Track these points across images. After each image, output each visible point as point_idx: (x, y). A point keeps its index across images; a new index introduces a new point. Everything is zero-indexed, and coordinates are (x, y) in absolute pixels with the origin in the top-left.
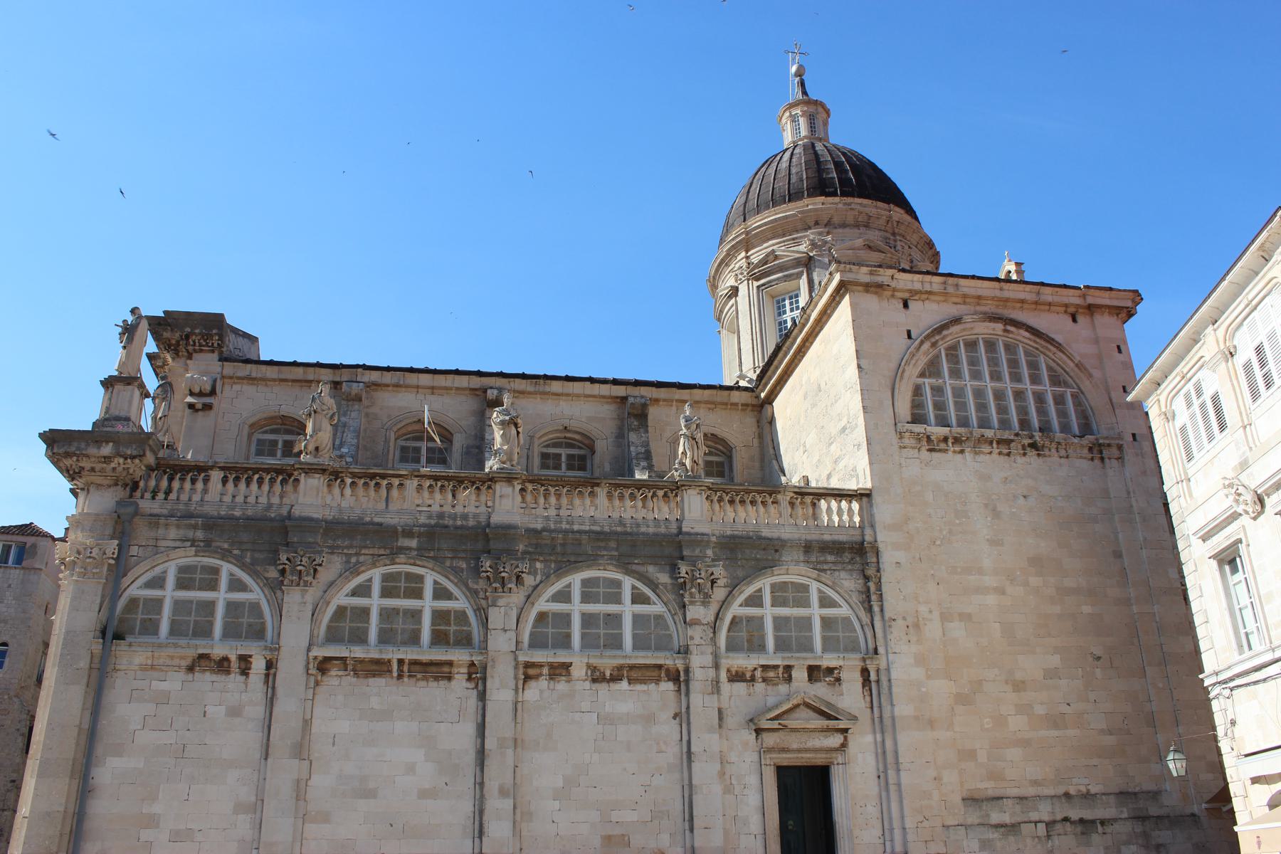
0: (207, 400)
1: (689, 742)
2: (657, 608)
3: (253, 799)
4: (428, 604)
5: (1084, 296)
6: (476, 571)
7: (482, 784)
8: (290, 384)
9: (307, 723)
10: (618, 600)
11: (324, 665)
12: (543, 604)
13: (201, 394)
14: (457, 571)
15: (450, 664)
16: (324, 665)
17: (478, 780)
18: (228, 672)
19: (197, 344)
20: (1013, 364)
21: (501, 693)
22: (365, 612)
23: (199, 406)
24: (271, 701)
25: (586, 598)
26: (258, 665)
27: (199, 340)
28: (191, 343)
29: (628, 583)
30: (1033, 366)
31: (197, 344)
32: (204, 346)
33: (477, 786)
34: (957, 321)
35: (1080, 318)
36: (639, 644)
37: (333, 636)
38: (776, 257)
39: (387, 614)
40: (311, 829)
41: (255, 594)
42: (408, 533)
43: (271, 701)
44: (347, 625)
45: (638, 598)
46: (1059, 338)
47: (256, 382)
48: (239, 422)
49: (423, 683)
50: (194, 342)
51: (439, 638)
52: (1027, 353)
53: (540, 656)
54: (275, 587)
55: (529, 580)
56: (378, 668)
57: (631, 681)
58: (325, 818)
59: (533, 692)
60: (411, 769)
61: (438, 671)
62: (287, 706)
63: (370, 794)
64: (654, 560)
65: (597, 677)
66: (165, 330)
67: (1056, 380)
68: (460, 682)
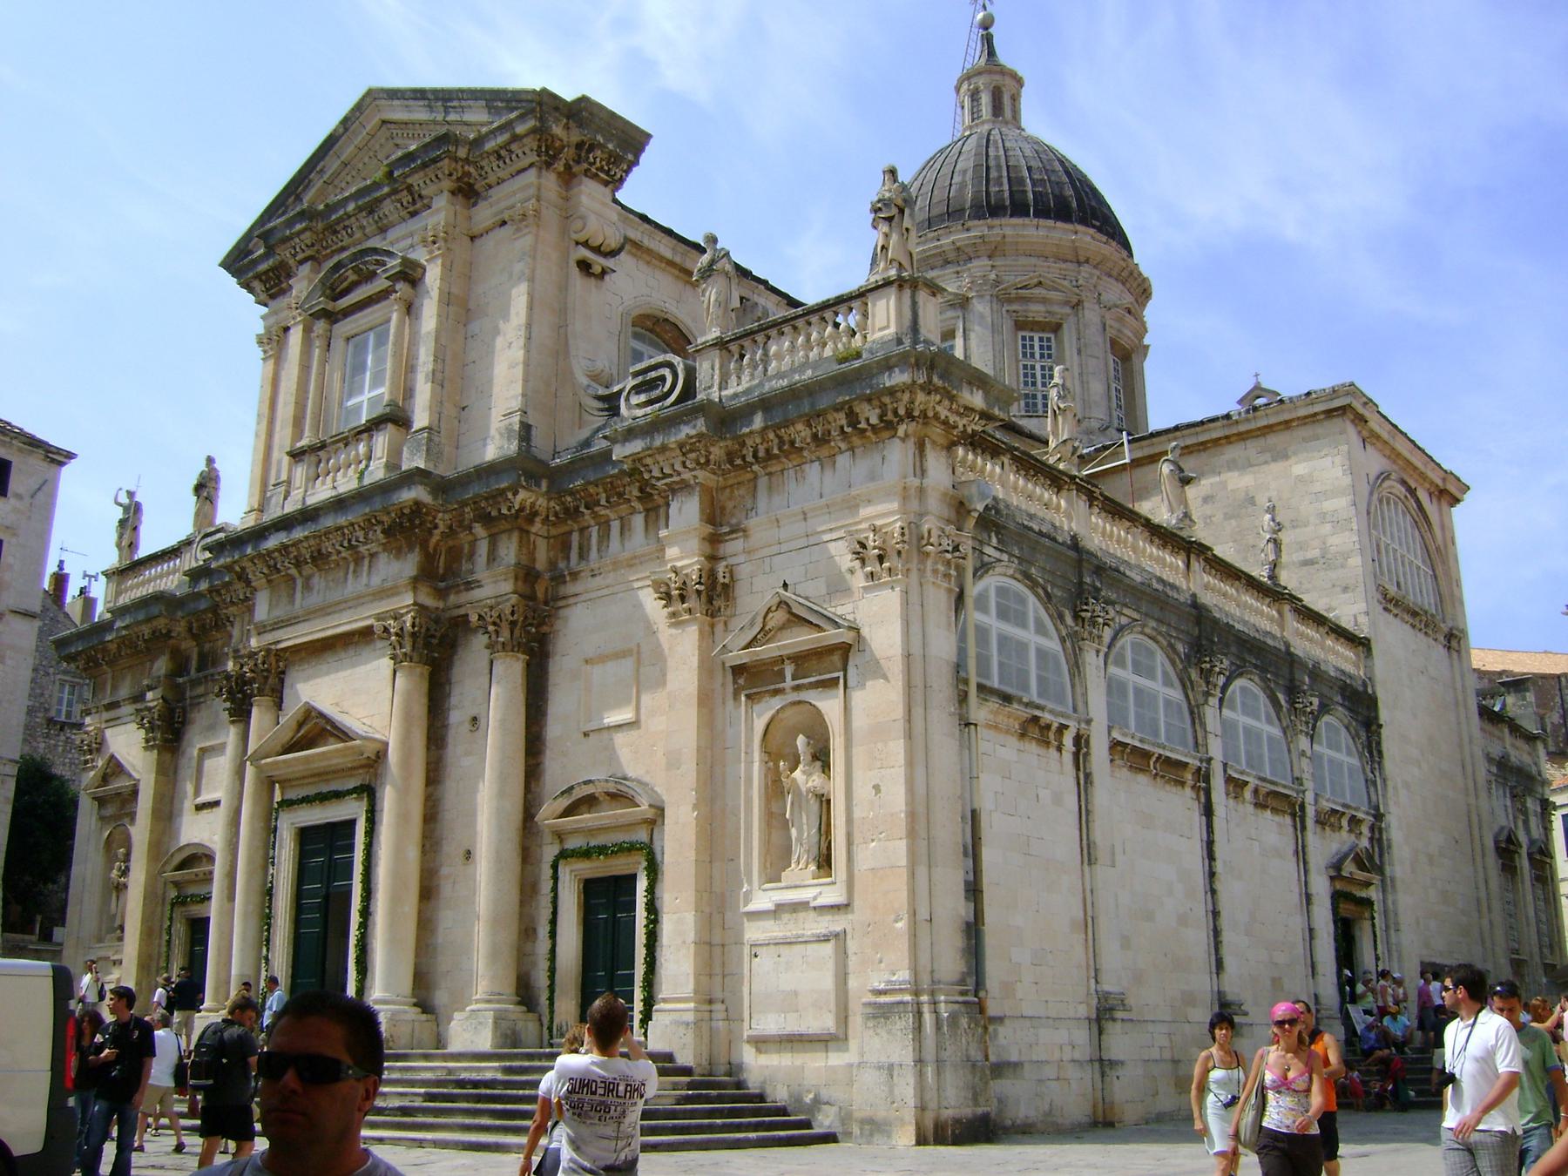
1: (1306, 882)
3: (1081, 914)
5: (1444, 480)
7: (1216, 914)
8: (677, 272)
13: (597, 250)
15: (1185, 765)
17: (1210, 907)
18: (1047, 744)
19: (598, 164)
23: (597, 269)
27: (602, 160)
28: (592, 160)
31: (598, 164)
32: (601, 169)
33: (1210, 915)
38: (1040, 284)
47: (639, 253)
48: (620, 309)
49: (1168, 787)
50: (595, 158)
57: (1275, 811)
66: (557, 121)
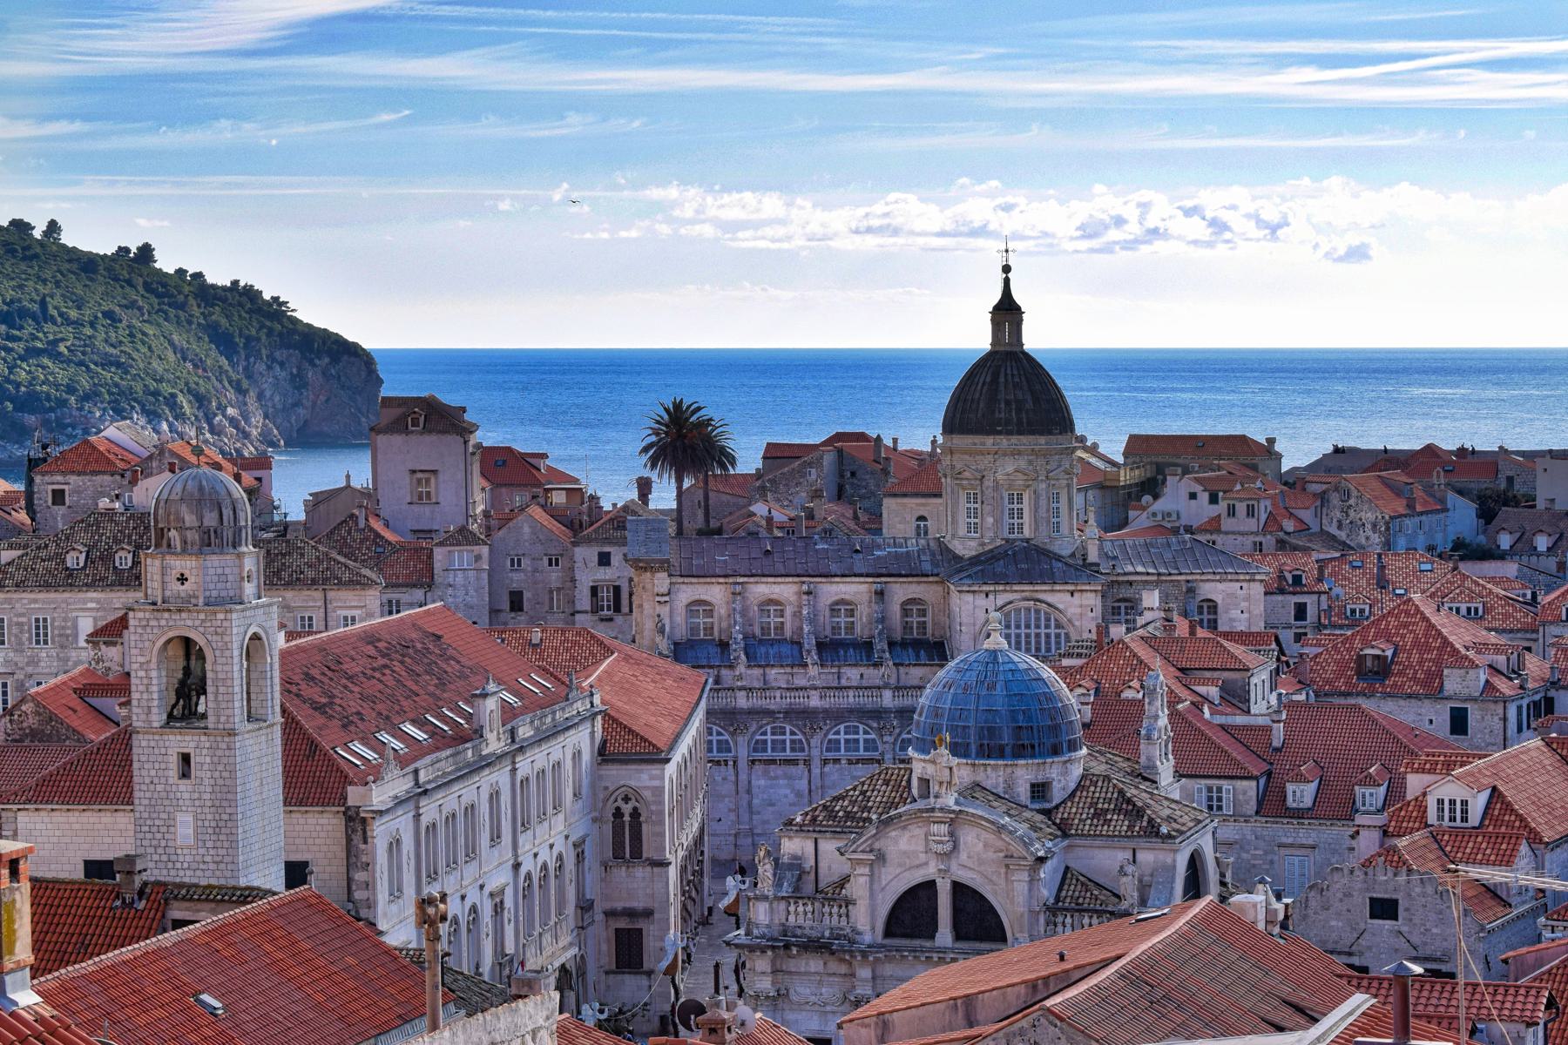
0: (667, 598)
2: (873, 736)
4: (788, 737)
6: (805, 726)
9: (750, 782)
10: (858, 733)
11: (753, 762)
12: (831, 736)
14: (797, 726)
16: (753, 762)
20: (1038, 619)
21: (816, 771)
22: (766, 741)
24: (737, 775)
25: (846, 733)
26: (731, 763)
29: (861, 727)
30: (1048, 619)
34: (1011, 602)
35: (1076, 594)
36: (866, 749)
37: (755, 750)
39: (773, 741)
40: (754, 817)
41: (726, 737)
42: (779, 712)
43: (737, 775)
44: (760, 746)
45: (866, 732)
46: (1061, 606)
51: (793, 750)
52: (1046, 613)
53: (830, 755)
54: (733, 734)
55: (825, 728)
56: (773, 762)
58: (759, 813)
59: (827, 769)
60: (786, 796)
61: (794, 762)
62: (743, 777)
63: (772, 805)
64: (871, 718)
65: (850, 762)
67: (1058, 626)
68: (801, 766)
